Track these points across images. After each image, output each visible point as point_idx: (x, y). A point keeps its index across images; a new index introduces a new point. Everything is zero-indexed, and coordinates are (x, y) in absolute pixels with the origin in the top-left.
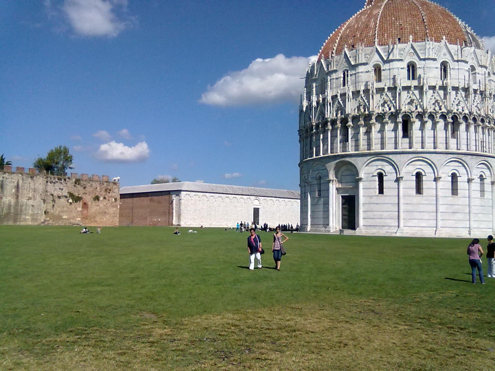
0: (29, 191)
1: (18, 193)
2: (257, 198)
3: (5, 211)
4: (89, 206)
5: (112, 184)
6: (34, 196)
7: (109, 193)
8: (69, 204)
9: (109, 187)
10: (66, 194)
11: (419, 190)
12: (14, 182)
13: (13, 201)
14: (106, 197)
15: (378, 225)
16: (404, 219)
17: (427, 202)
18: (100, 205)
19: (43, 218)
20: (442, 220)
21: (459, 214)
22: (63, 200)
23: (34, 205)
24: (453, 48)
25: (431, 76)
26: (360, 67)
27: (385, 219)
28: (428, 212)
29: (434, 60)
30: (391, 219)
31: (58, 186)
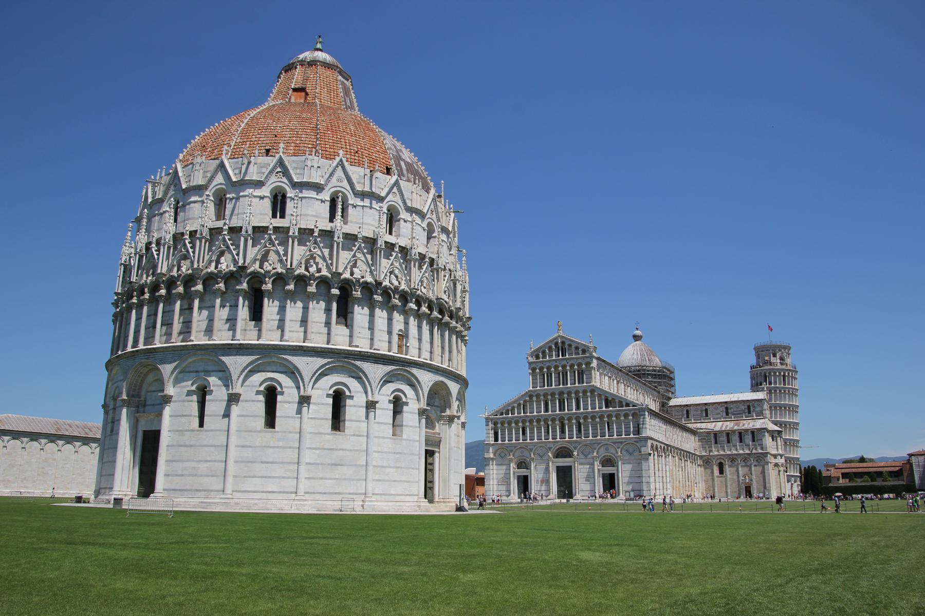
11: (271, 421)
15: (188, 487)
16: (235, 476)
17: (281, 444)
20: (309, 478)
21: (345, 467)
24: (356, 172)
25: (310, 213)
27: (201, 476)
28: (282, 463)
29: (318, 188)
30: (212, 476)
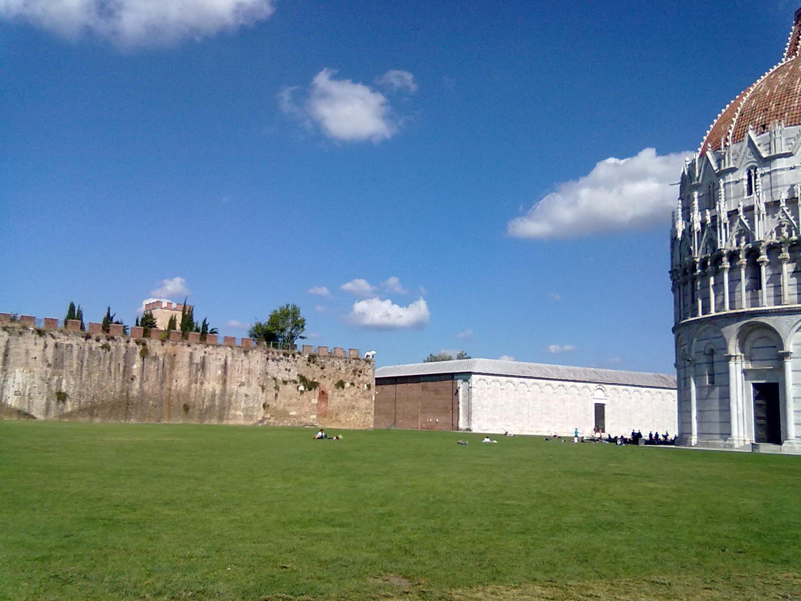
0: (241, 373)
1: (225, 376)
2: (601, 387)
3: (207, 403)
4: (329, 397)
5: (364, 362)
6: (249, 381)
7: (359, 376)
8: (299, 393)
9: (360, 368)
10: (295, 378)
12: (220, 359)
13: (218, 388)
14: (355, 382)
18: (346, 395)
19: (260, 414)
22: (290, 387)
23: (248, 393)
26: (778, 160)
31: (283, 364)
